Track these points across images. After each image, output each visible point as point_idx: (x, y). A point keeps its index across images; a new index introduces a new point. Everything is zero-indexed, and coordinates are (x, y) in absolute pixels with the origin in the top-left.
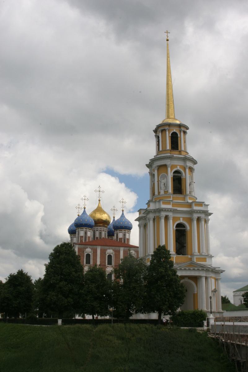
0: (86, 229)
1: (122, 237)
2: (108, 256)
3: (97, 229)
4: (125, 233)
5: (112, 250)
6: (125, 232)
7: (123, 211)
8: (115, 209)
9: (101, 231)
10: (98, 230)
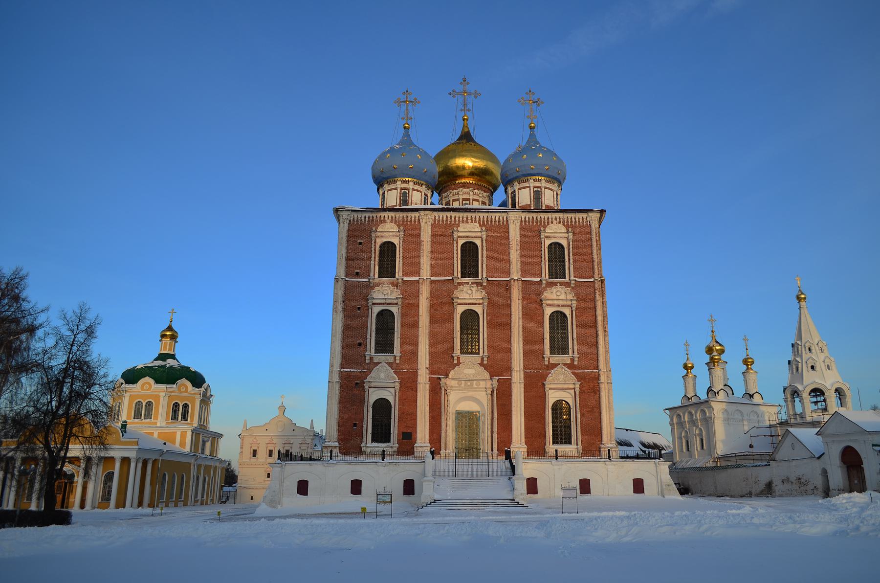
0: (403, 182)
2: (462, 246)
3: (456, 198)
4: (540, 187)
5: (478, 225)
7: (531, 128)
10: (458, 200)
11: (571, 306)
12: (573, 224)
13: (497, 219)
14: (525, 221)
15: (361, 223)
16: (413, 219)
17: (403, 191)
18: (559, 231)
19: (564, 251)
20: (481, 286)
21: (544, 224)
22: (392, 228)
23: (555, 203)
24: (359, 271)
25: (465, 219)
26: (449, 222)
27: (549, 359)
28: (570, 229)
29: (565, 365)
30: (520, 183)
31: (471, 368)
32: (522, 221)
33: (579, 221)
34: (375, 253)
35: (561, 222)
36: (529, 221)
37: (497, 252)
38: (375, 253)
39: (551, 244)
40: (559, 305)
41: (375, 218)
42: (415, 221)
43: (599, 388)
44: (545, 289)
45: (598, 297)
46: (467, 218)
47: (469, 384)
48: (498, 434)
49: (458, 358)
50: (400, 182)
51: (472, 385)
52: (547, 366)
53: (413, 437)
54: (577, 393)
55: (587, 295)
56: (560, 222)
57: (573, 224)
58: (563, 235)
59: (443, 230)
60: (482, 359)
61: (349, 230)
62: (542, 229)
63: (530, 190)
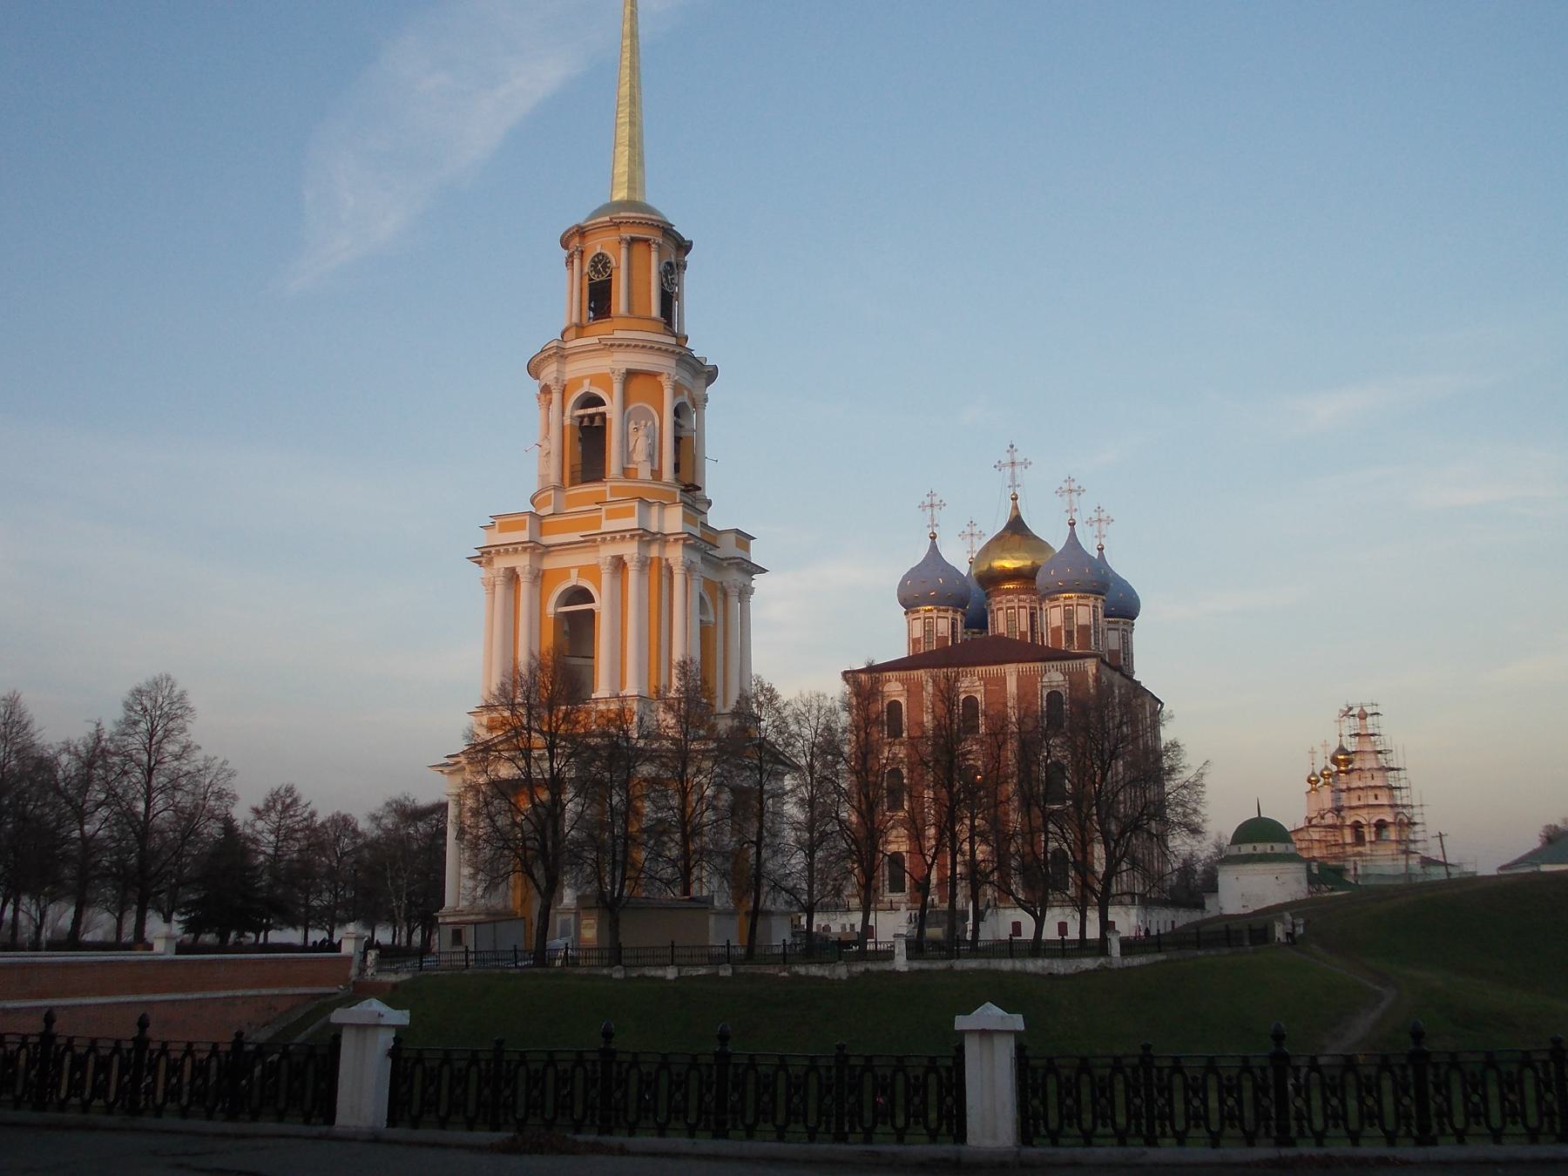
1: (1060, 624)
2: (963, 700)
3: (1000, 606)
4: (1072, 605)
6: (1068, 602)
7: (1072, 524)
8: (1103, 515)
9: (1013, 608)
10: (1002, 609)
14: (1023, 671)
22: (898, 687)
23: (1092, 619)
32: (1019, 672)
56: (1057, 670)
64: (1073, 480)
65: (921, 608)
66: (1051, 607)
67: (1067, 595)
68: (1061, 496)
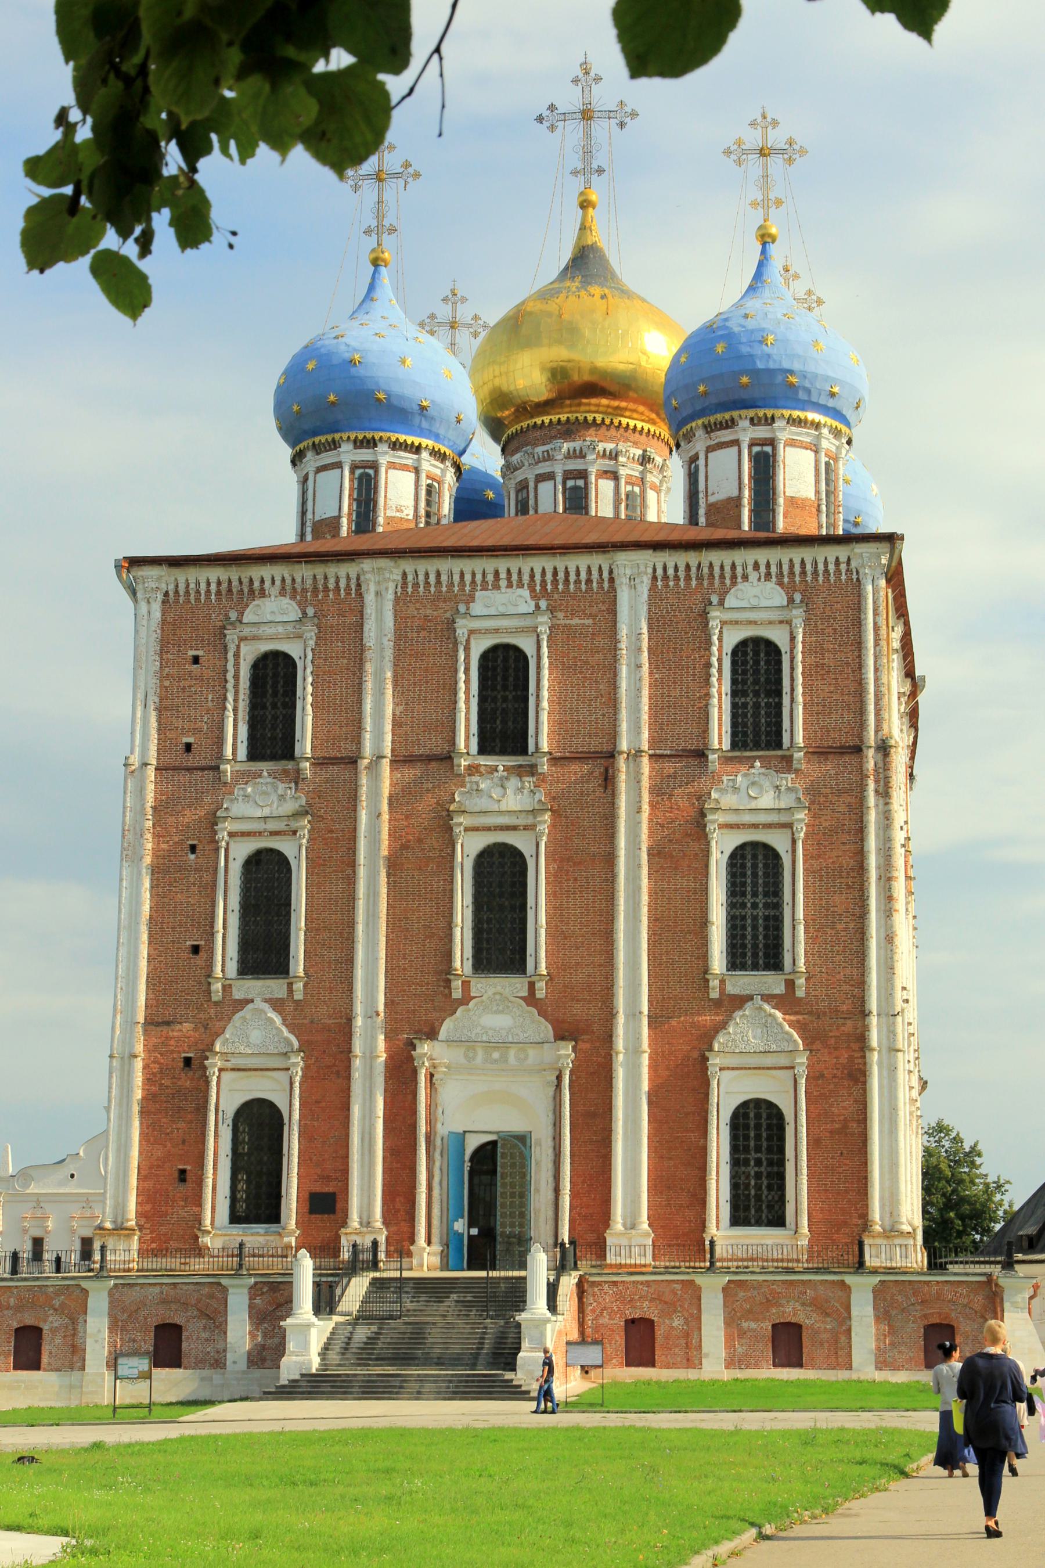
0: (359, 444)
1: (736, 493)
3: (543, 468)
5: (526, 593)
6: (762, 432)
10: (550, 476)
11: (789, 826)
12: (809, 578)
13: (583, 576)
14: (665, 577)
15: (198, 600)
16: (343, 584)
17: (358, 472)
18: (764, 603)
19: (779, 662)
20: (533, 775)
21: (723, 583)
24: (191, 740)
25: (490, 578)
26: (444, 589)
27: (722, 982)
28: (798, 597)
29: (767, 998)
30: (712, 431)
31: (502, 1012)
32: (654, 578)
33: (826, 571)
34: (236, 687)
35: (773, 574)
36: (677, 578)
37: (581, 673)
38: (236, 687)
39: (743, 644)
40: (755, 826)
41: (235, 583)
42: (348, 587)
43: (865, 1064)
44: (716, 779)
45: (871, 799)
46: (497, 573)
47: (496, 1055)
48: (573, 1196)
49: (466, 985)
50: (351, 446)
51: (504, 1059)
52: (718, 1003)
53: (339, 1205)
54: (803, 1082)
55: (840, 793)
56: (768, 575)
57: (809, 578)
58: (774, 616)
59: (429, 612)
60: (532, 986)
61: (164, 621)
62: (715, 599)
63: (740, 452)
64: (775, 123)
65: (345, 437)
66: (709, 449)
67: (761, 413)
68: (739, 162)
